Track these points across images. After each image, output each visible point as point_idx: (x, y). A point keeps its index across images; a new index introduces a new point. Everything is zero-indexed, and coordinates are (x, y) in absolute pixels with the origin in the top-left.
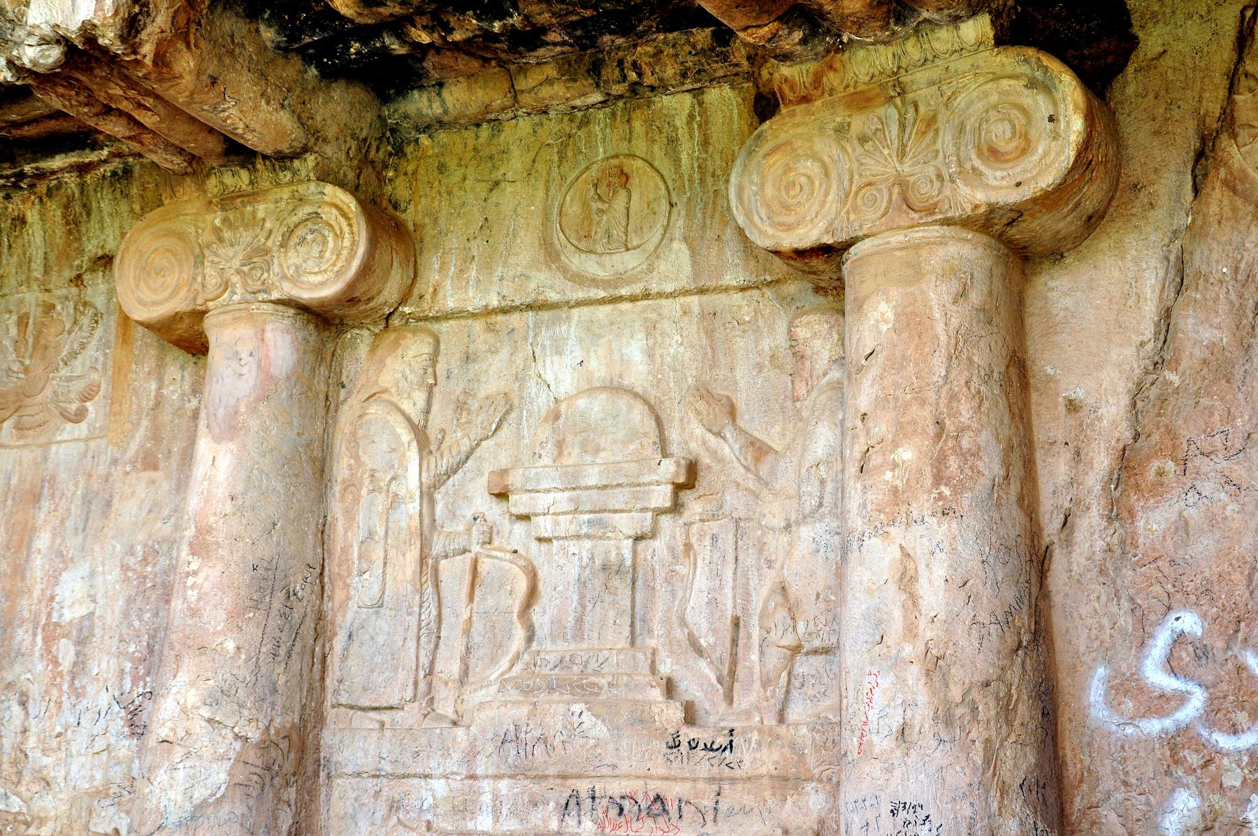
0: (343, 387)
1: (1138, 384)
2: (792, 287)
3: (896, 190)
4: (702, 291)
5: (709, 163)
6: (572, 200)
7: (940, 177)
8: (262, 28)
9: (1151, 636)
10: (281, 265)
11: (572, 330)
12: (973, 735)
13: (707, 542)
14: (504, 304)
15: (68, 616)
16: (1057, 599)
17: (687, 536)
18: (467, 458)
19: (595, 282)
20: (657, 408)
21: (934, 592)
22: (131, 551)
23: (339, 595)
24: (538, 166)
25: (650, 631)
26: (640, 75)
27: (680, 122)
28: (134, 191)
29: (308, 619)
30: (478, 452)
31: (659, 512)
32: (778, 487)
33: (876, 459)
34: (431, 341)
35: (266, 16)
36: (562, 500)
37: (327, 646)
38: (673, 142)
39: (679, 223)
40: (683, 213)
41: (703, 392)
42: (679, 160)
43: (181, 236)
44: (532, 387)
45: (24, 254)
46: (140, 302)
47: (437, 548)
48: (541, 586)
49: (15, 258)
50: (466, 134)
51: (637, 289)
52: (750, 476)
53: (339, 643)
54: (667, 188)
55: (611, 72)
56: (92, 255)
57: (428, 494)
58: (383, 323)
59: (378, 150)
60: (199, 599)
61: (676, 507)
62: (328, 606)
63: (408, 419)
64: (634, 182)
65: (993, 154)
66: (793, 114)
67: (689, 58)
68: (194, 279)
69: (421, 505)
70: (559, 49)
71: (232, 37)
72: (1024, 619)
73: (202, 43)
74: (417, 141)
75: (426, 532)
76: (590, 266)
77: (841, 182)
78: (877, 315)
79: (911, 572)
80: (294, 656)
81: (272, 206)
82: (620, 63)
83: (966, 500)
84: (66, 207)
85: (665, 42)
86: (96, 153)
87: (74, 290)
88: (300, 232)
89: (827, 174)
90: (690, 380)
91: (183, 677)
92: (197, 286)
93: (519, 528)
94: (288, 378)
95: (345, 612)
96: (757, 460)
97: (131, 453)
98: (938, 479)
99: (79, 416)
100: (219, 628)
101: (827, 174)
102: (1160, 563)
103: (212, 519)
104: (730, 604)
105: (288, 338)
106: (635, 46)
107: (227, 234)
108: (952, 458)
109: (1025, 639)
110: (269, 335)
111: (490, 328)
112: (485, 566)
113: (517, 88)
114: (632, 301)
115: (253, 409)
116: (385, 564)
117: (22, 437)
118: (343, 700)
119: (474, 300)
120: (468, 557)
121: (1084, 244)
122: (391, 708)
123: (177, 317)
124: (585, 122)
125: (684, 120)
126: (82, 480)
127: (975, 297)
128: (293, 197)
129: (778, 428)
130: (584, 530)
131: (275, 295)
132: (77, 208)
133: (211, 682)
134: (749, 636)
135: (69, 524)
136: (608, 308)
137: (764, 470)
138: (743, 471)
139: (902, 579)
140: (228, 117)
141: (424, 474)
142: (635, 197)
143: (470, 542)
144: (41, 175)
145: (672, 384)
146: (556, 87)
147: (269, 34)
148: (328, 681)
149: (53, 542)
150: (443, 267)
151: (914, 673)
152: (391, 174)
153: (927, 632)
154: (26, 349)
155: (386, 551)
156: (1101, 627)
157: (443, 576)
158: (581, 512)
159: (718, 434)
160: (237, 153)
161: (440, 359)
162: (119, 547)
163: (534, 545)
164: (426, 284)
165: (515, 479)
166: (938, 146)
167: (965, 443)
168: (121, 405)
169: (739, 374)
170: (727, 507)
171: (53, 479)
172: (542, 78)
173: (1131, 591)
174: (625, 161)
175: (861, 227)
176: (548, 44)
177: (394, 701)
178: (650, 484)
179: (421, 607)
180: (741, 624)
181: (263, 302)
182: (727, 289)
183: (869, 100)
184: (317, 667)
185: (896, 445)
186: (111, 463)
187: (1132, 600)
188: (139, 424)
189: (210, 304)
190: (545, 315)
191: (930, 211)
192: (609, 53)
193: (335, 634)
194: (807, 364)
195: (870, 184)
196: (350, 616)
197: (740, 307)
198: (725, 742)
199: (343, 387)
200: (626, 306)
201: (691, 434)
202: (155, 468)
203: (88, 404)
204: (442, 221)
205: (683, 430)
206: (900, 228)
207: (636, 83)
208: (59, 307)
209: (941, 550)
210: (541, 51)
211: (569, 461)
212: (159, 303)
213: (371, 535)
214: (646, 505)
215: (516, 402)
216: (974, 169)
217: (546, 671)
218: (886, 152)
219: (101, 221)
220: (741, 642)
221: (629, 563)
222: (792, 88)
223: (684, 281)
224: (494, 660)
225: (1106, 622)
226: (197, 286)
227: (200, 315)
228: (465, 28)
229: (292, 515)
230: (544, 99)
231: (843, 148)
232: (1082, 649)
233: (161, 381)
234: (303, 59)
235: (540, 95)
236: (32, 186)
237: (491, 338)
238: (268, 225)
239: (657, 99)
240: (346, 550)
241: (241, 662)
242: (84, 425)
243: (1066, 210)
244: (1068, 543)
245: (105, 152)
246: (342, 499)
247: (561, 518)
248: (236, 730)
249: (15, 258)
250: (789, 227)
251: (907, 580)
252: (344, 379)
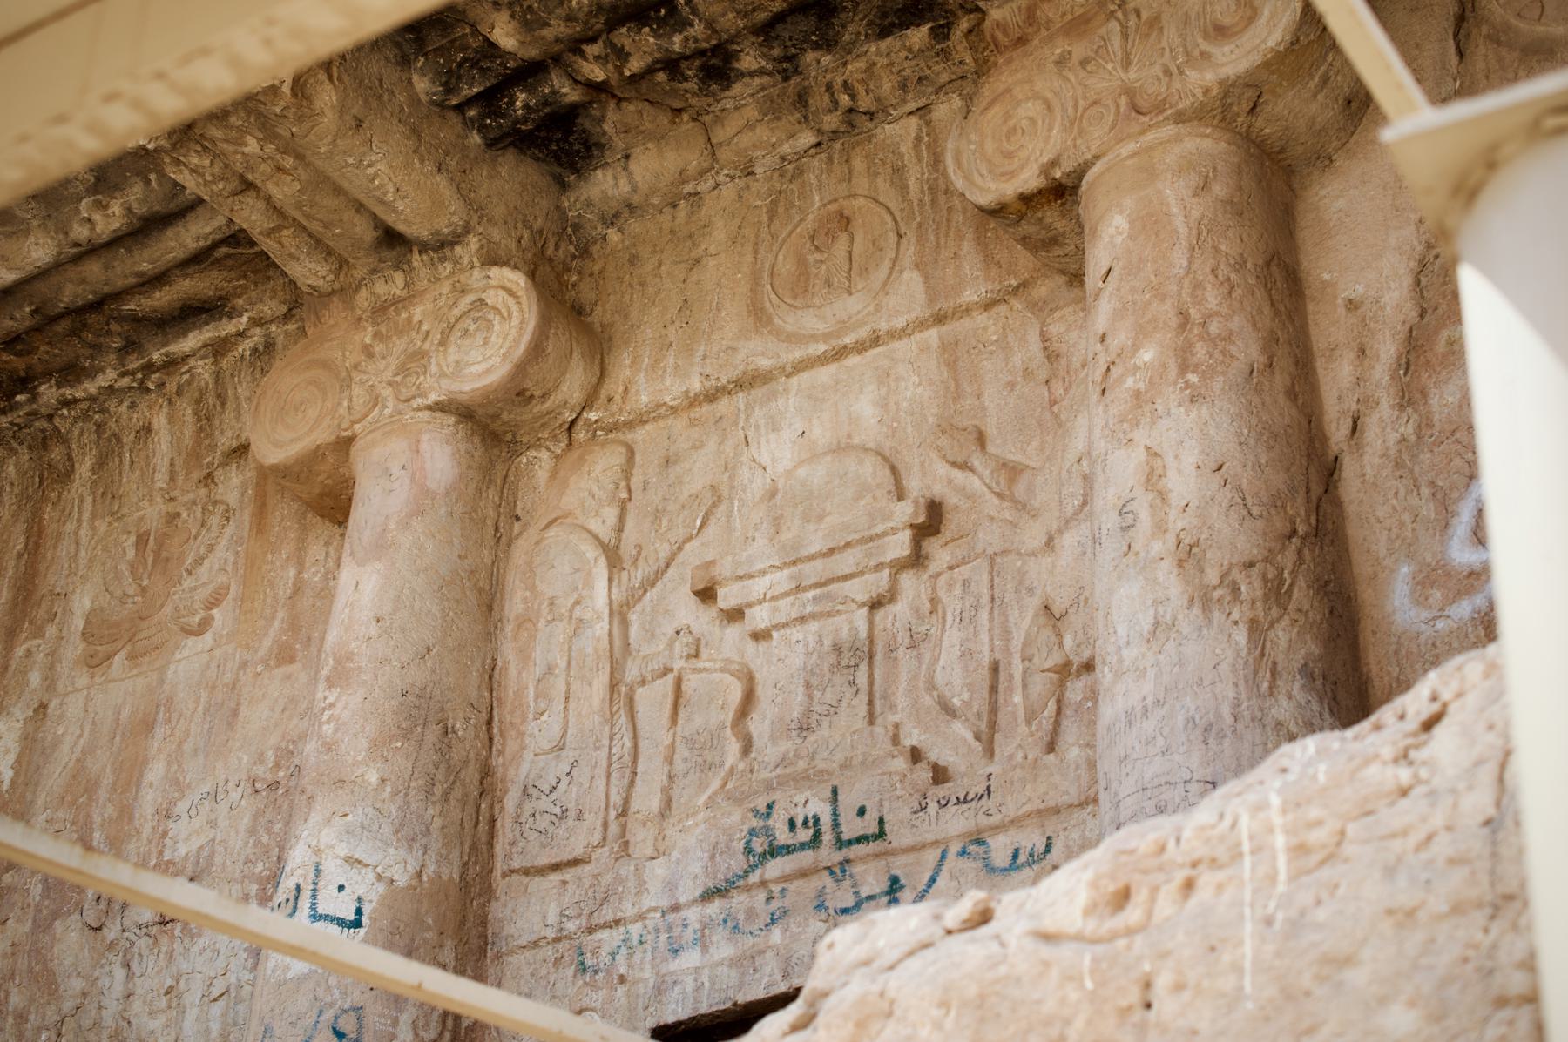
0: (518, 519)
1: (1420, 261)
2: (1043, 289)
3: (1123, 101)
4: (940, 319)
5: (941, 181)
6: (785, 258)
7: (1167, 72)
8: (415, 78)
9: (1454, 514)
10: (438, 364)
11: (791, 401)
12: (1235, 615)
13: (958, 590)
14: (707, 384)
15: (182, 850)
16: (1351, 509)
17: (934, 589)
18: (668, 566)
19: (814, 338)
20: (892, 459)
21: (1185, 481)
22: (261, 759)
23: (512, 746)
24: (748, 231)
25: (893, 707)
26: (853, 97)
27: (906, 148)
29: (471, 767)
30: (680, 558)
31: (900, 566)
32: (1036, 504)
33: (1116, 372)
34: (623, 450)
35: (420, 64)
36: (781, 580)
37: (497, 807)
38: (898, 171)
39: (909, 251)
40: (913, 240)
41: (946, 428)
42: (907, 187)
43: (326, 365)
44: (744, 473)
45: (148, 465)
46: (277, 445)
47: (632, 672)
48: (759, 691)
49: (138, 473)
50: (661, 218)
51: (863, 333)
52: (1006, 504)
53: (510, 801)
54: (895, 219)
55: (819, 100)
56: (226, 448)
57: (619, 614)
58: (565, 437)
59: (557, 247)
60: (336, 731)
61: (917, 559)
62: (497, 761)
63: (596, 538)
64: (857, 223)
65: (1220, 32)
66: (1009, 61)
67: (907, 64)
68: (340, 404)
69: (611, 623)
70: (757, 81)
71: (381, 81)
72: (1298, 508)
73: (346, 78)
74: (604, 238)
75: (617, 655)
76: (810, 321)
77: (1064, 109)
78: (1112, 231)
79: (1159, 471)
80: (453, 802)
81: (429, 306)
82: (829, 87)
83: (1218, 383)
84: (198, 402)
85: (878, 53)
87: (203, 492)
88: (459, 326)
89: (1049, 108)
90: (930, 420)
91: (316, 818)
92: (342, 411)
93: (733, 632)
94: (447, 493)
95: (518, 765)
96: (1012, 481)
97: (261, 653)
98: (1184, 369)
100: (360, 758)
101: (1049, 108)
102: (1458, 435)
103: (354, 644)
104: (986, 649)
105: (448, 449)
106: (845, 64)
107: (378, 348)
108: (1199, 345)
109: (1301, 529)
110: (424, 446)
111: (693, 423)
112: (691, 683)
113: (714, 141)
114: (860, 352)
115: (405, 525)
116: (567, 698)
117: (137, 666)
118: (516, 865)
119: (672, 389)
120: (670, 678)
121: (1352, 140)
122: (575, 862)
123: (316, 455)
124: (799, 173)
125: (910, 144)
126: (204, 695)
127: (1219, 190)
128: (454, 290)
129: (1035, 444)
130: (809, 609)
131: (433, 398)
132: (211, 400)
133: (349, 818)
134: (1011, 676)
135: (188, 747)
136: (832, 368)
137: (1020, 490)
138: (996, 501)
139: (1148, 480)
140: (376, 176)
141: (615, 590)
142: (858, 238)
143: (672, 658)
144: (172, 364)
145: (909, 430)
146: (758, 130)
147: (422, 85)
148: (498, 848)
149: (168, 770)
150: (635, 361)
151: (1167, 574)
152: (574, 279)
153: (1177, 522)
154: (145, 569)
155: (568, 684)
156: (1402, 525)
157: (642, 708)
158: (805, 589)
159: (964, 466)
160: (392, 239)
161: (634, 471)
162: (245, 758)
163: (751, 646)
164: (613, 386)
165: (724, 568)
166: (1164, 44)
167: (1214, 328)
168: (253, 601)
169: (986, 399)
170: (979, 548)
171: (170, 700)
172: (742, 123)
173: (1430, 475)
174: (846, 203)
175: (1088, 148)
176: (743, 75)
177: (579, 852)
178: (885, 534)
179: (611, 739)
180: (1001, 668)
181: (419, 409)
182: (967, 311)
183: (1088, 21)
184: (483, 826)
185: (1136, 348)
186: (239, 668)
187: (1432, 483)
188: (273, 618)
189: (357, 427)
190: (758, 393)
191: (1160, 107)
192: (816, 78)
193: (506, 792)
194: (1063, 361)
195: (1095, 103)
196: (525, 767)
197: (985, 329)
198: (981, 789)
199: (518, 519)
200: (853, 360)
201: (932, 476)
202: (292, 660)
203: (215, 612)
204: (634, 314)
205: (924, 473)
206: (1129, 136)
207: (851, 110)
208: (184, 515)
209: (1191, 438)
210: (737, 88)
211: (786, 536)
212: (298, 439)
213: (550, 670)
214: (882, 560)
215: (726, 494)
216: (1202, 54)
217: (765, 775)
218: (1109, 66)
219: (238, 410)
220: (1001, 688)
221: (863, 634)
222: (1005, 33)
223: (919, 310)
224: (702, 786)
225: (1407, 517)
226: (342, 411)
227: (344, 444)
228: (642, 47)
229: (450, 642)
230: (746, 150)
231: (1066, 79)
232: (1383, 552)
234: (464, 123)
235: (742, 146)
236: (161, 385)
237: (695, 433)
238: (425, 327)
239: (879, 130)
240: (519, 694)
241: (386, 795)
242: (208, 638)
243: (1312, 84)
244: (1359, 447)
245: (245, 319)
246: (515, 638)
247: (781, 603)
248: (379, 870)
249: (138, 473)
250: (1011, 175)
251: (1153, 479)
252: (519, 511)
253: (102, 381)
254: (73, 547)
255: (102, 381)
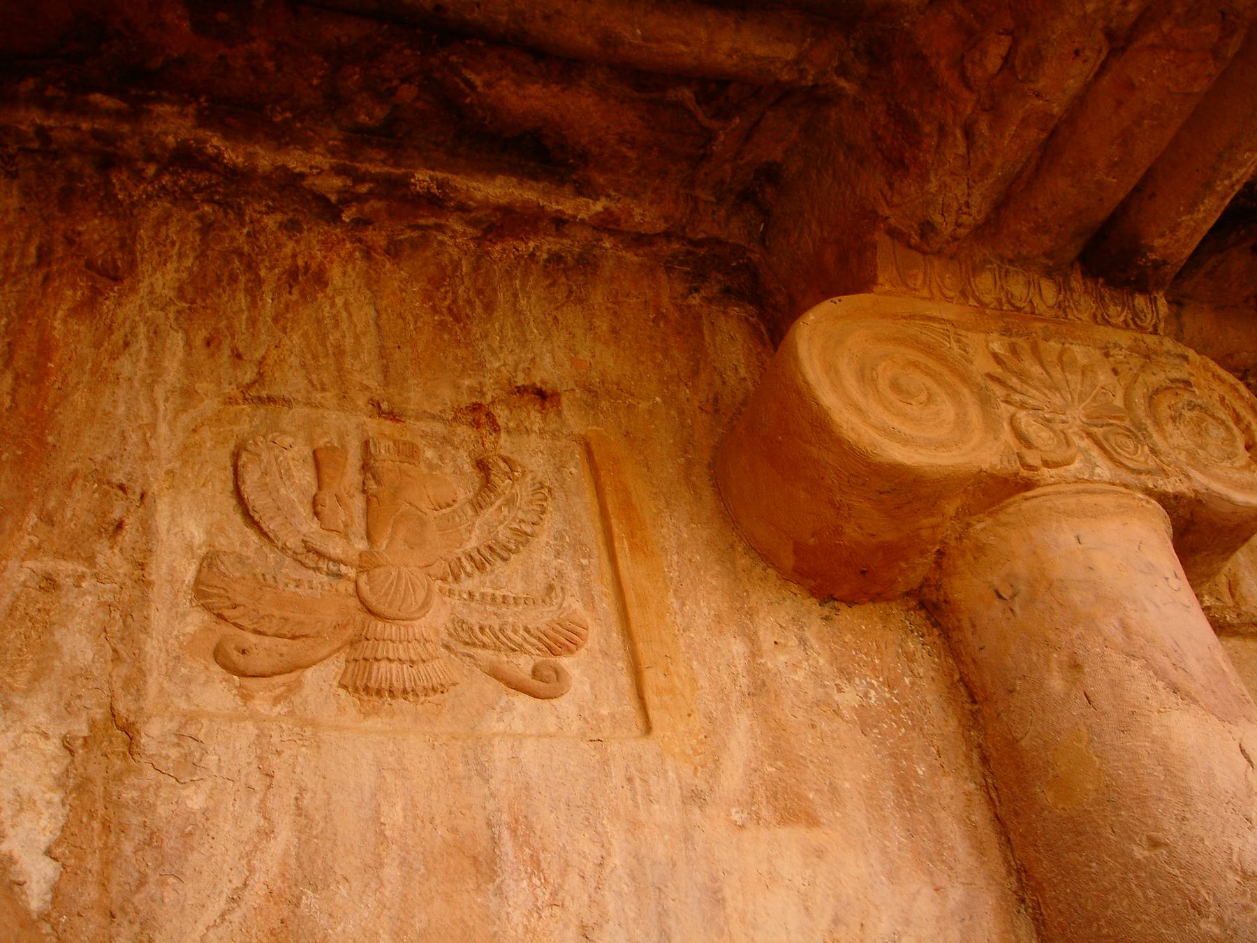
28: (598, 297)
86: (581, 200)
99: (545, 684)
189: (1046, 471)
203: (565, 661)
233: (752, 640)
242: (565, 705)
253: (295, 160)
254: (145, 409)
255: (295, 160)
